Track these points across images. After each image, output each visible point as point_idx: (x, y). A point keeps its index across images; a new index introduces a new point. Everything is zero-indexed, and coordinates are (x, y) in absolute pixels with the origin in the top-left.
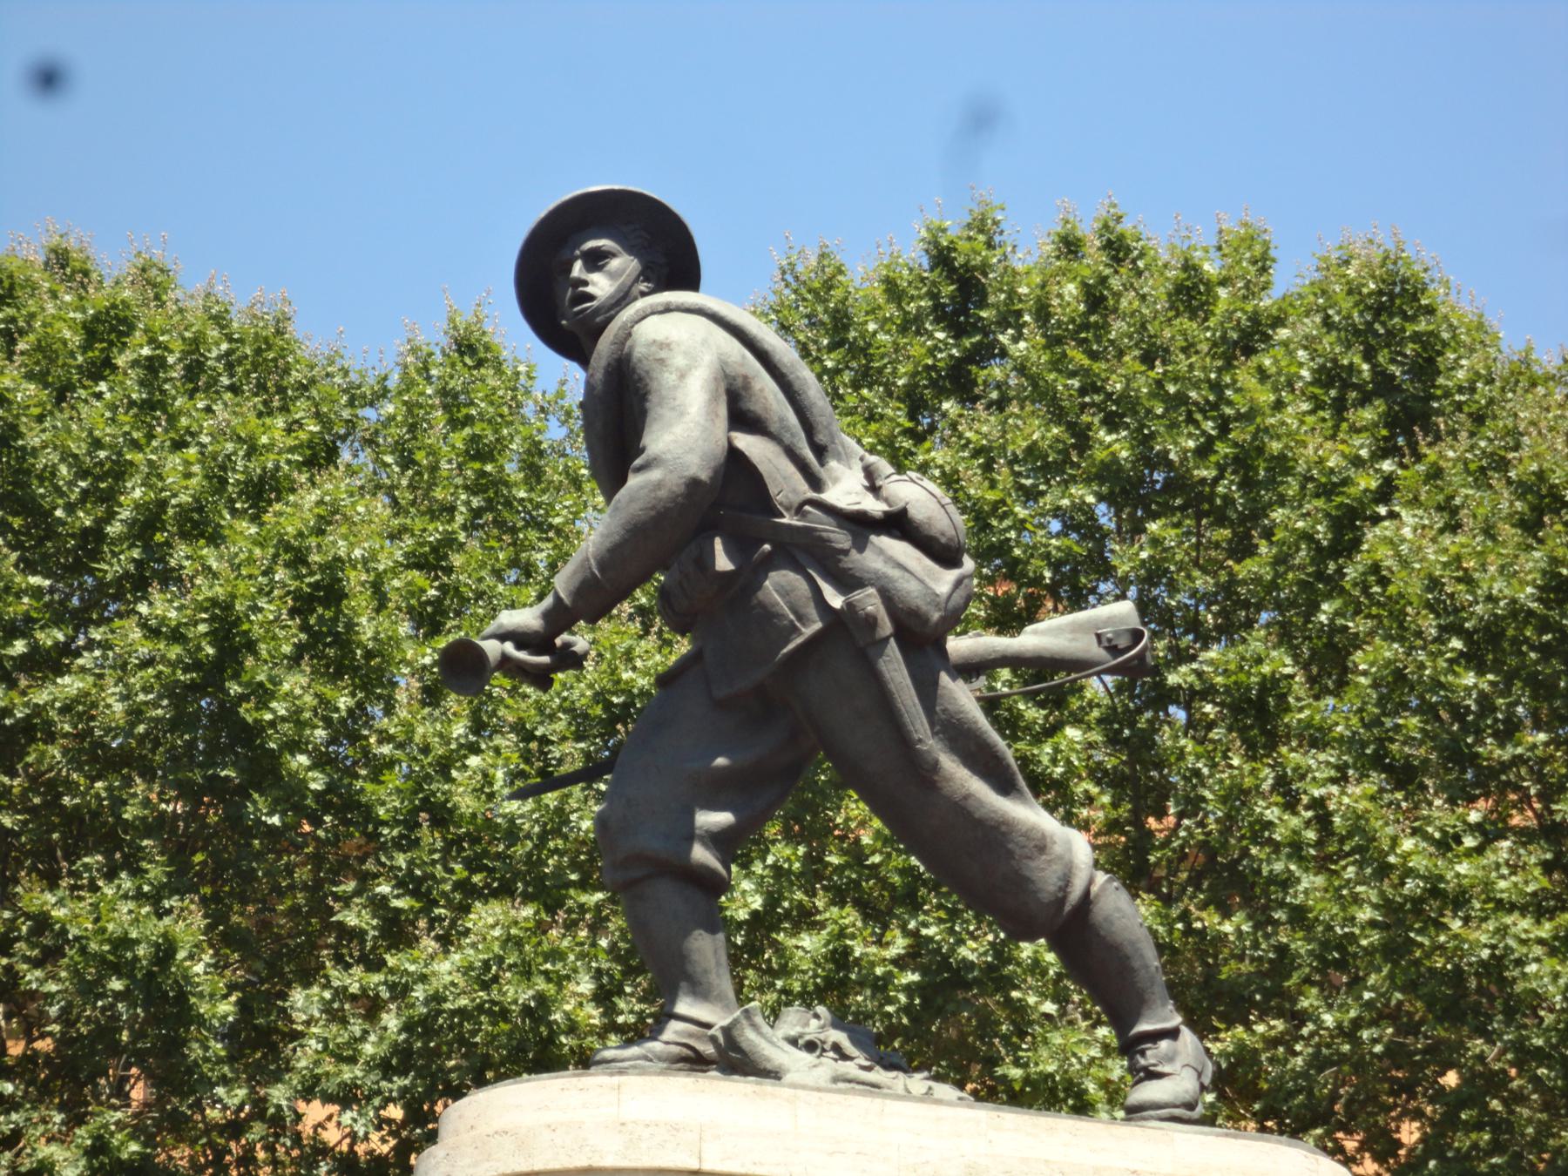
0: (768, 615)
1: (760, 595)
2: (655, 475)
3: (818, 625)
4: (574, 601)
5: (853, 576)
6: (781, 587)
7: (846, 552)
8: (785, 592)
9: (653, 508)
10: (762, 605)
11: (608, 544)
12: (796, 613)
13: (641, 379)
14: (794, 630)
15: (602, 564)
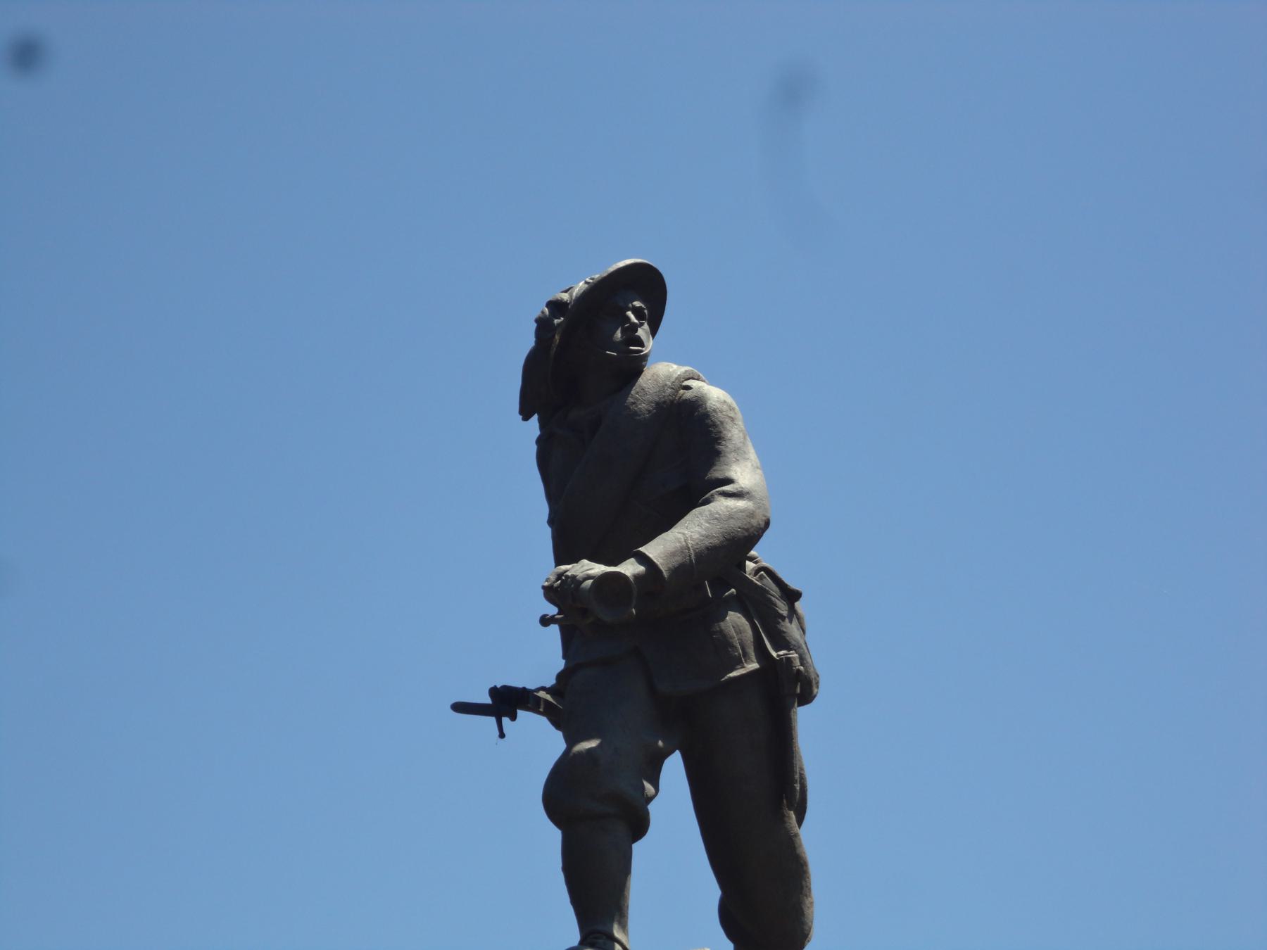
0: (724, 643)
1: (722, 624)
2: (741, 504)
3: (753, 666)
4: (670, 576)
5: (784, 639)
6: (735, 621)
7: (783, 618)
8: (739, 632)
9: (747, 530)
10: (721, 631)
11: (707, 543)
12: (743, 649)
13: (714, 425)
14: (738, 663)
15: (699, 555)
